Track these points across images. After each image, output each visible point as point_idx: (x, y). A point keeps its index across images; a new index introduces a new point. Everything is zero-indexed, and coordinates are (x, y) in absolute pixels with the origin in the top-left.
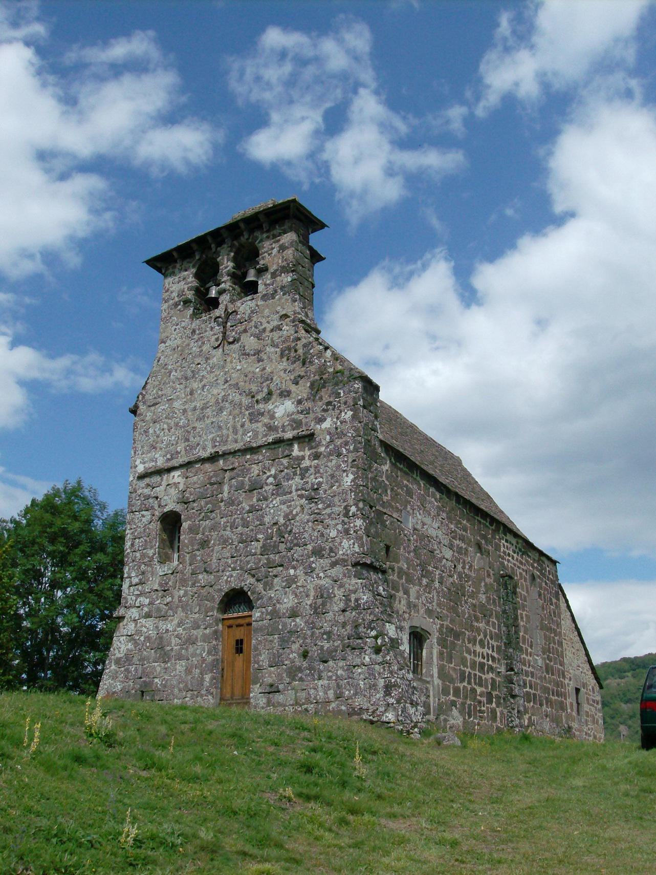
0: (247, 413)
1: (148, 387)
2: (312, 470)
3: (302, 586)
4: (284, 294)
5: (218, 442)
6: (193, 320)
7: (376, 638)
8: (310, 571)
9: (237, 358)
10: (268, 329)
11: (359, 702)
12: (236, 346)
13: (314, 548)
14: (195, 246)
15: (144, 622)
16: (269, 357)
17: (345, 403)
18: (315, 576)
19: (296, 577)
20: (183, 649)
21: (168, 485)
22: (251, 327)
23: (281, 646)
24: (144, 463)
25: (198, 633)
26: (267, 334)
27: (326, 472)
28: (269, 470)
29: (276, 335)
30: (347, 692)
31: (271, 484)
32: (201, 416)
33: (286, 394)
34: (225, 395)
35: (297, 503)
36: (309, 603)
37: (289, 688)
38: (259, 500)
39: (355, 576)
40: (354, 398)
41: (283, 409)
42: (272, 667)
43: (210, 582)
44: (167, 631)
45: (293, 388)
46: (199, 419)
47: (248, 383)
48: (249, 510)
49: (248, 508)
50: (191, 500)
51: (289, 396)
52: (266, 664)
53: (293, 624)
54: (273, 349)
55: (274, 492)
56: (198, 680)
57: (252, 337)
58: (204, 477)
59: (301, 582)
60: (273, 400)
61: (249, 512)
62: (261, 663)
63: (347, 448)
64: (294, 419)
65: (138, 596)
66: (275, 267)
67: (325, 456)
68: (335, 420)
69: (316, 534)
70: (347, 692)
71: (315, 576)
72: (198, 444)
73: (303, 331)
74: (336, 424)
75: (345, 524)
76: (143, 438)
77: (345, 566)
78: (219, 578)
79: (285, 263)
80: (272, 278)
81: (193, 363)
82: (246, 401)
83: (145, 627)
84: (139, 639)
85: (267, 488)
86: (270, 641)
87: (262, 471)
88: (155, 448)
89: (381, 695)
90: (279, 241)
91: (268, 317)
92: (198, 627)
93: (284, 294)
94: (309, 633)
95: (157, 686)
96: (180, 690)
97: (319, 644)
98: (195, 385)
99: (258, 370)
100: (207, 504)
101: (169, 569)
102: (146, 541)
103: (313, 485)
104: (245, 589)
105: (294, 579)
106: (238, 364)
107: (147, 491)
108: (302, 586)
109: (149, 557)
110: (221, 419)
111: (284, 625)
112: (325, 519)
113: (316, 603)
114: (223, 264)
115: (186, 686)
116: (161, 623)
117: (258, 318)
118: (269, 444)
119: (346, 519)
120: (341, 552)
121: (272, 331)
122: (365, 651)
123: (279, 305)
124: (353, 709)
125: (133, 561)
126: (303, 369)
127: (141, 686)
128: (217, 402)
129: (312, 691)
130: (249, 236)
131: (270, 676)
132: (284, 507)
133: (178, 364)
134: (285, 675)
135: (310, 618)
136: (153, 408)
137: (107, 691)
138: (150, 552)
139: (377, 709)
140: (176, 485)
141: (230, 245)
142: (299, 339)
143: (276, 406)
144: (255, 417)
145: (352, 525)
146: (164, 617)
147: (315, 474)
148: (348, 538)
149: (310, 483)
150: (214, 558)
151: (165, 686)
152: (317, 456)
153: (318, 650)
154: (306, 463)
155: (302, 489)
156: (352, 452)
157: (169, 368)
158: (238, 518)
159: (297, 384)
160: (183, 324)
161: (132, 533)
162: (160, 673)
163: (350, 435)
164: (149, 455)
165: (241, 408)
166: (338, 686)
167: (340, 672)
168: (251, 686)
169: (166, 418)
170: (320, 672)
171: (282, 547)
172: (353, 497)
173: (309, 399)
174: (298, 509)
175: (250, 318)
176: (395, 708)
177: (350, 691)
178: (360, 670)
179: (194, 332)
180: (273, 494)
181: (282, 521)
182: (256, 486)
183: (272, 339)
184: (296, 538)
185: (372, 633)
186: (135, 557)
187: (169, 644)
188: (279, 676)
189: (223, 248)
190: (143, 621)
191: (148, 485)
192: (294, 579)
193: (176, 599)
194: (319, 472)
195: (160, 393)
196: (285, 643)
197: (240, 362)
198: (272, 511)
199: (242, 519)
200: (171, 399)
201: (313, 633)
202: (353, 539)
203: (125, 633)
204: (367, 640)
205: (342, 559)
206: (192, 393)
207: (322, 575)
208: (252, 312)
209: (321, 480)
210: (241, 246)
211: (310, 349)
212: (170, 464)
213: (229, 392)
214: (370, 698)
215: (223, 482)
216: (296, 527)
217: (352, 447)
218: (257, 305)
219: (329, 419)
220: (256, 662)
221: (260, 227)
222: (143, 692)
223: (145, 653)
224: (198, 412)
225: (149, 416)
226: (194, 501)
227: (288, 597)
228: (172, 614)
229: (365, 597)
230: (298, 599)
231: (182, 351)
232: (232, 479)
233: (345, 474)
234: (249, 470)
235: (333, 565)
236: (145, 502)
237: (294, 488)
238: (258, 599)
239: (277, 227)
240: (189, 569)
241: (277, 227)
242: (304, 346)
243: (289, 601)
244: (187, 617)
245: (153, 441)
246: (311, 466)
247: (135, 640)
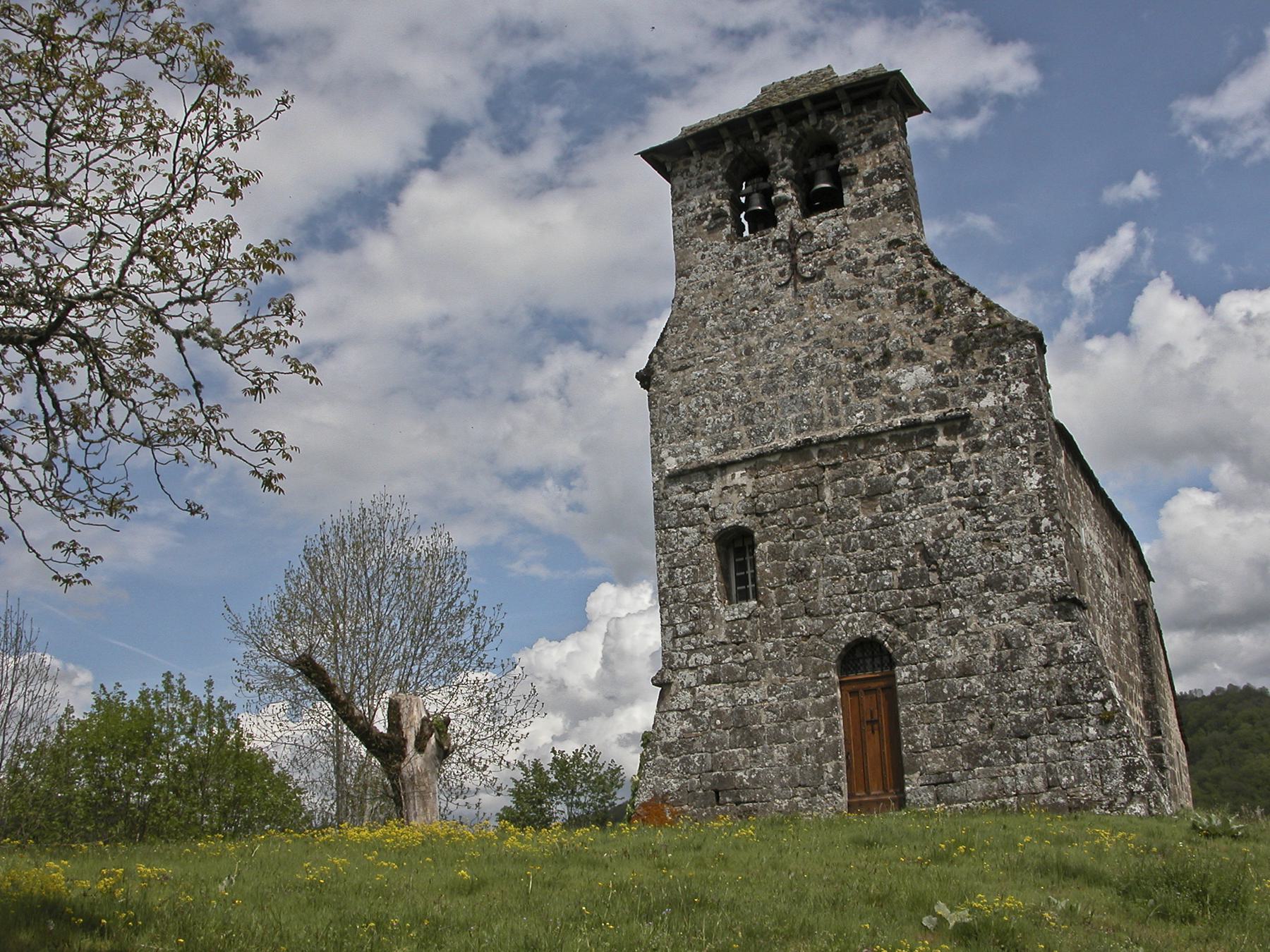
0: (851, 383)
1: (667, 341)
2: (972, 467)
3: (977, 633)
4: (889, 210)
5: (806, 425)
6: (733, 242)
7: (1103, 702)
8: (985, 610)
9: (822, 301)
10: (871, 262)
11: (1084, 791)
12: (818, 284)
13: (988, 578)
14: (725, 133)
15: (706, 690)
16: (878, 303)
17: (1015, 371)
18: (994, 618)
19: (964, 620)
20: (782, 727)
21: (724, 489)
22: (842, 257)
23: (949, 717)
24: (676, 455)
25: (809, 703)
26: (870, 267)
27: (996, 470)
28: (900, 467)
29: (885, 270)
30: (1065, 779)
31: (905, 486)
32: (770, 386)
33: (914, 356)
34: (809, 356)
35: (953, 514)
36: (988, 656)
37: (970, 776)
38: (886, 510)
39: (1059, 618)
40: (1028, 365)
41: (913, 378)
42: (938, 747)
43: (818, 630)
44: (750, 701)
45: (926, 348)
46: (767, 391)
47: (846, 339)
48: (872, 524)
49: (869, 522)
50: (768, 510)
51: (920, 359)
52: (927, 743)
53: (965, 686)
54: (882, 291)
55: (912, 498)
56: (813, 772)
57: (844, 272)
58: (788, 477)
59: (972, 626)
60: (893, 365)
61: (872, 526)
62: (918, 743)
63: (1026, 435)
64: (933, 393)
65: (690, 652)
66: (869, 169)
67: (990, 447)
68: (1001, 395)
69: (989, 558)
70: (1065, 779)
71: (994, 618)
72: (770, 429)
73: (930, 266)
74: (1003, 400)
75: (1036, 544)
76: (669, 418)
77: (1041, 603)
78: (833, 623)
79: (885, 164)
80: (866, 184)
81: (744, 307)
82: (847, 366)
83: (710, 697)
84: (700, 715)
85: (899, 493)
86: (931, 711)
87: (888, 468)
88: (694, 433)
89: (1119, 780)
90: (870, 130)
91: (867, 242)
92: (806, 695)
93: (889, 210)
94: (994, 698)
95: (742, 782)
96: (783, 786)
97: (1012, 712)
98: (753, 341)
99: (861, 320)
100: (797, 515)
101: (741, 612)
102: (694, 570)
103: (975, 488)
104: (879, 637)
105: (961, 623)
106: (825, 310)
107: (687, 497)
108: (977, 633)
109: (703, 595)
110: (806, 392)
111: (952, 689)
112: (1002, 537)
113: (1000, 655)
114: (775, 161)
115: (793, 779)
116: (737, 691)
117: (850, 244)
118: (896, 428)
119: (1036, 537)
120: (1033, 584)
121: (877, 263)
122: (1087, 722)
123: (884, 226)
124: (1078, 801)
125: (676, 601)
126: (938, 321)
127: (714, 783)
128: (796, 367)
129: (1008, 780)
130: (818, 121)
131: (935, 760)
132: (931, 521)
133: (719, 308)
134: (960, 758)
135: (992, 677)
136: (680, 374)
137: (654, 792)
138: (706, 588)
139: (1116, 800)
140: (739, 488)
141: (785, 133)
142: (926, 277)
143: (899, 374)
144: (864, 390)
145: (1046, 545)
146: (743, 682)
147: (977, 473)
148: (1042, 564)
149: (970, 485)
150: (821, 594)
151: (755, 781)
152: (978, 447)
153: (1011, 722)
154: (961, 457)
155: (959, 494)
156: (1033, 441)
157: (702, 313)
158: (853, 536)
159: (931, 342)
160: (716, 249)
161: (668, 560)
162: (744, 763)
163: (1029, 417)
164: (683, 443)
165: (839, 376)
166: (1049, 769)
167: (1050, 751)
168: (906, 776)
169: (706, 388)
170: (1017, 752)
171: (934, 577)
172: (1044, 505)
173: (954, 364)
174: (956, 522)
175: (836, 243)
176: (1143, 797)
177: (1069, 777)
178: (1082, 748)
179: (737, 261)
180: (910, 502)
181: (929, 539)
182: (876, 492)
183: (880, 275)
184: (957, 564)
185: (1096, 695)
186: (679, 594)
187: (756, 719)
188: (951, 760)
189: (772, 137)
190: (706, 688)
191: (687, 489)
192: (961, 623)
194: (983, 470)
195: (690, 351)
196: (954, 712)
197: (828, 307)
198: (912, 526)
199: (862, 537)
200: (711, 361)
201: (1000, 700)
202: (1049, 564)
203: (676, 707)
204: (1089, 705)
205: (1037, 593)
206: (748, 351)
207: (1005, 615)
208: (838, 234)
209: (989, 481)
210: (804, 134)
211: (948, 292)
212: (725, 457)
213: (816, 351)
214: (1102, 785)
215: (822, 484)
216: (954, 548)
217: (1033, 436)
218: (846, 225)
219: (990, 395)
220: (909, 742)
221: (836, 108)
222: (717, 792)
223: (714, 734)
224: (763, 381)
225: (675, 385)
226: (774, 512)
227: (954, 648)
228: (756, 677)
229: (1079, 647)
230: (970, 651)
231: (721, 289)
232: (836, 479)
233: (1026, 473)
234: (864, 466)
235: (1022, 601)
236: (687, 513)
237: (944, 492)
238: (903, 652)
239: (865, 110)
240: (776, 611)
241: (865, 110)
242: (936, 287)
243: (955, 654)
244: (783, 681)
245: (689, 423)
246: (969, 461)
247: (694, 716)
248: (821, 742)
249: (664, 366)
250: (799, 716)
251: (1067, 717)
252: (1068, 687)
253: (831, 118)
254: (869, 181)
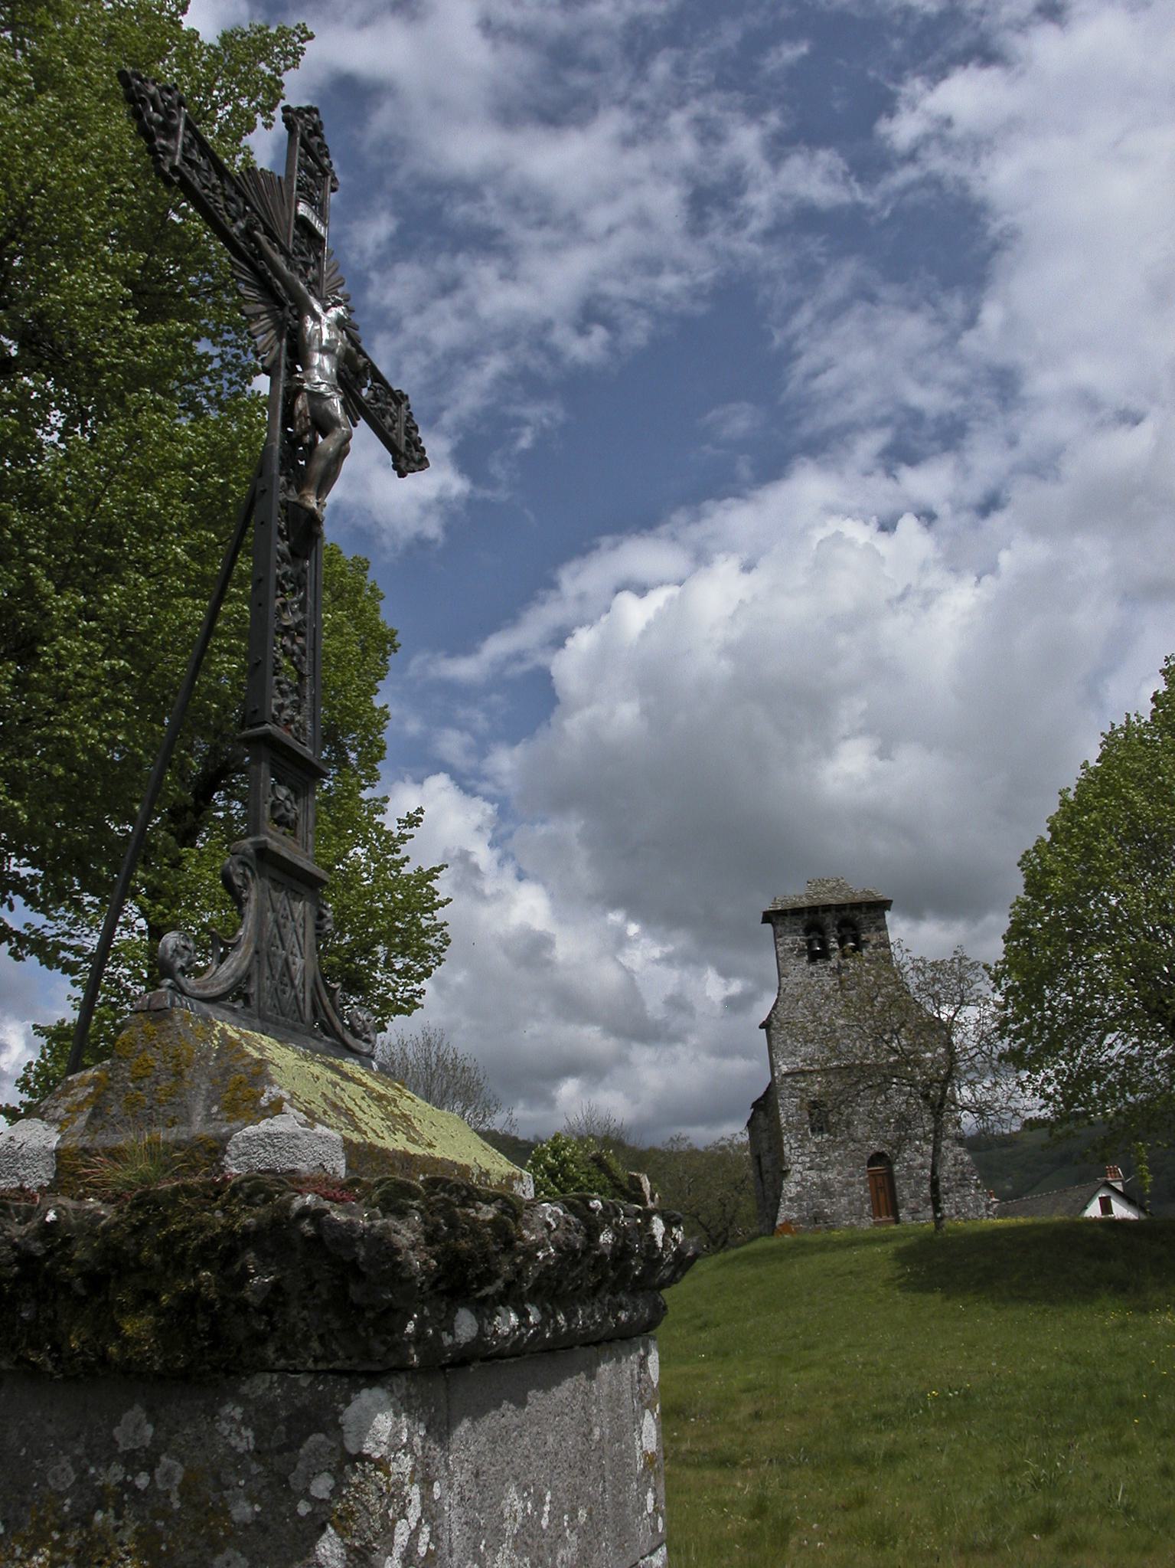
11: (970, 1214)
25: (855, 1180)
89: (984, 1210)
92: (854, 1176)
111: (917, 1174)
116: (823, 1174)
146: (825, 1170)
187: (833, 1186)
188: (918, 1203)
193: (833, 1158)
248: (862, 1196)
249: (778, 1021)
250: (852, 1185)
251: (963, 1186)
252: (963, 1174)
253: (856, 912)
254: (875, 947)
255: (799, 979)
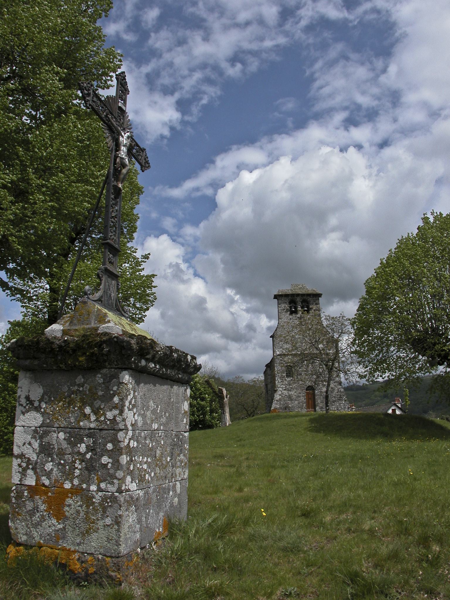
89: (347, 409)
138: (284, 375)
146: (290, 391)
193: (293, 387)
235: (335, 383)
250: (300, 397)
251: (340, 400)
252: (340, 395)
253: (308, 297)
254: (314, 310)
255: (286, 320)
